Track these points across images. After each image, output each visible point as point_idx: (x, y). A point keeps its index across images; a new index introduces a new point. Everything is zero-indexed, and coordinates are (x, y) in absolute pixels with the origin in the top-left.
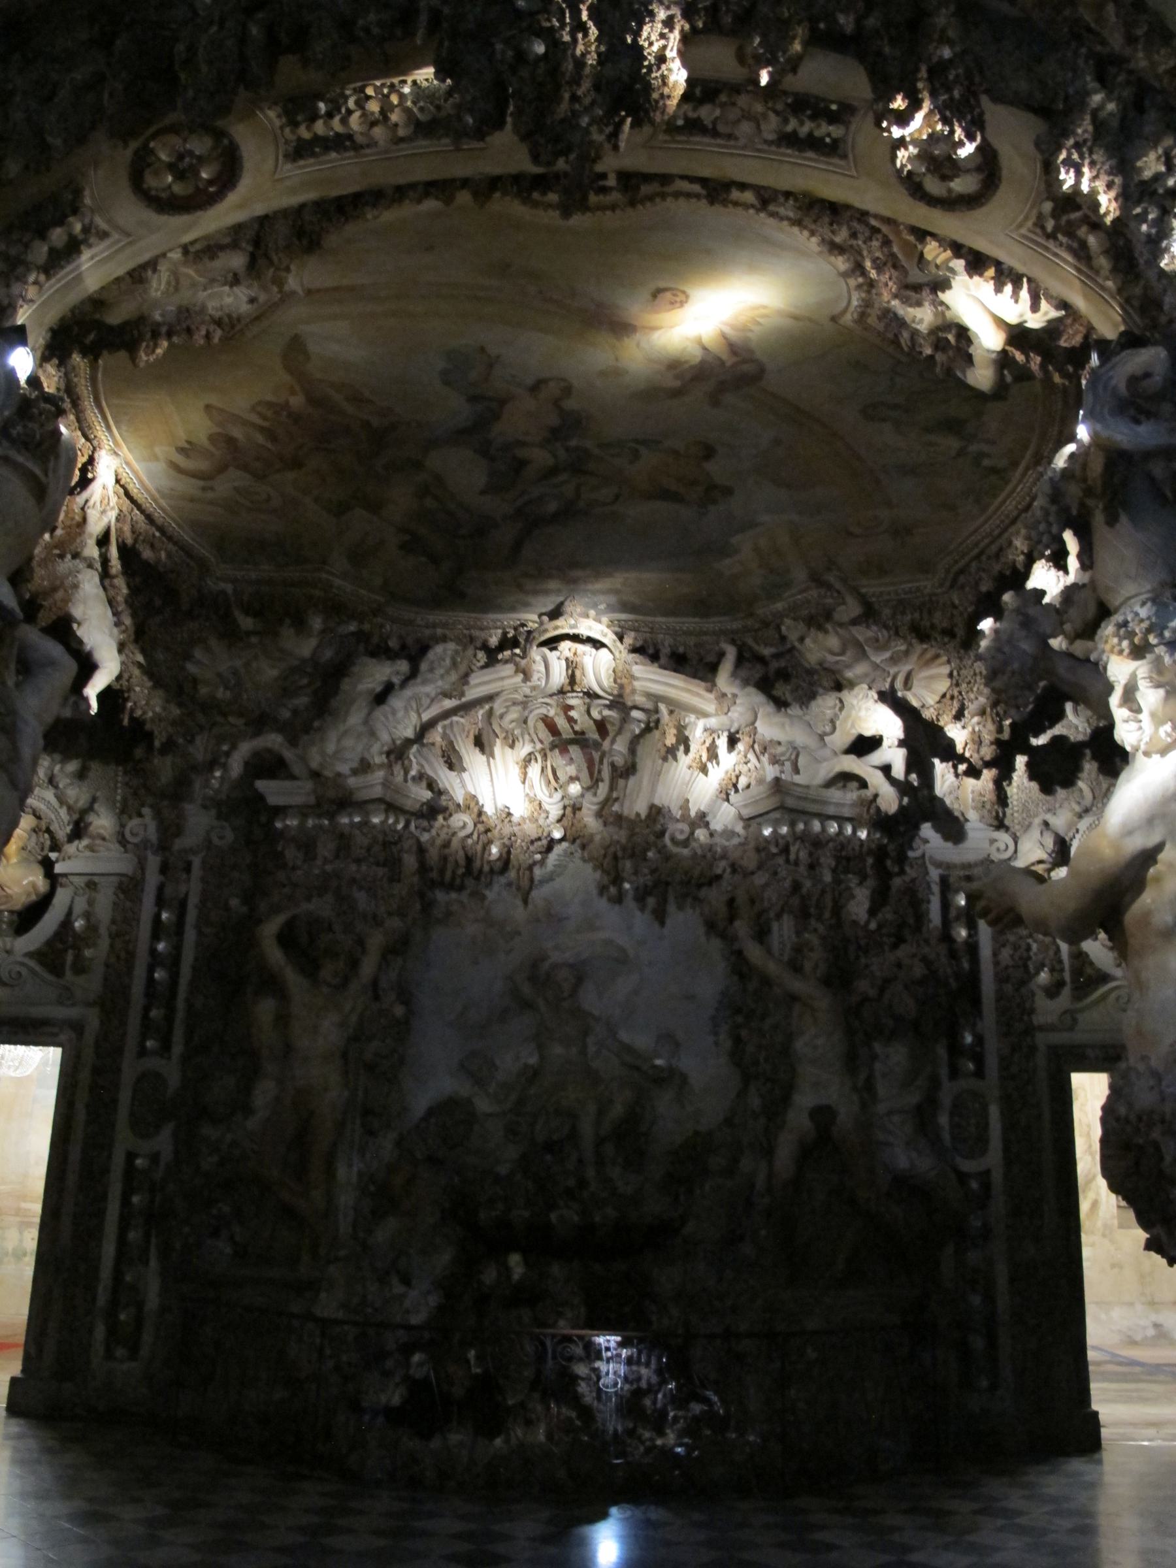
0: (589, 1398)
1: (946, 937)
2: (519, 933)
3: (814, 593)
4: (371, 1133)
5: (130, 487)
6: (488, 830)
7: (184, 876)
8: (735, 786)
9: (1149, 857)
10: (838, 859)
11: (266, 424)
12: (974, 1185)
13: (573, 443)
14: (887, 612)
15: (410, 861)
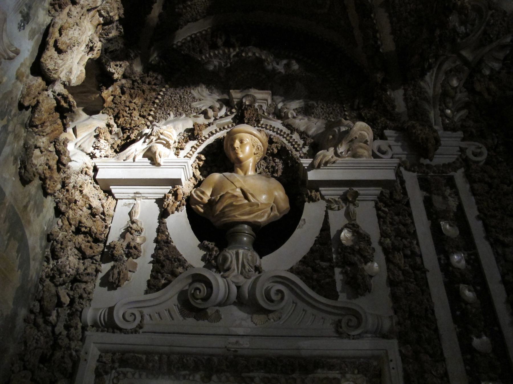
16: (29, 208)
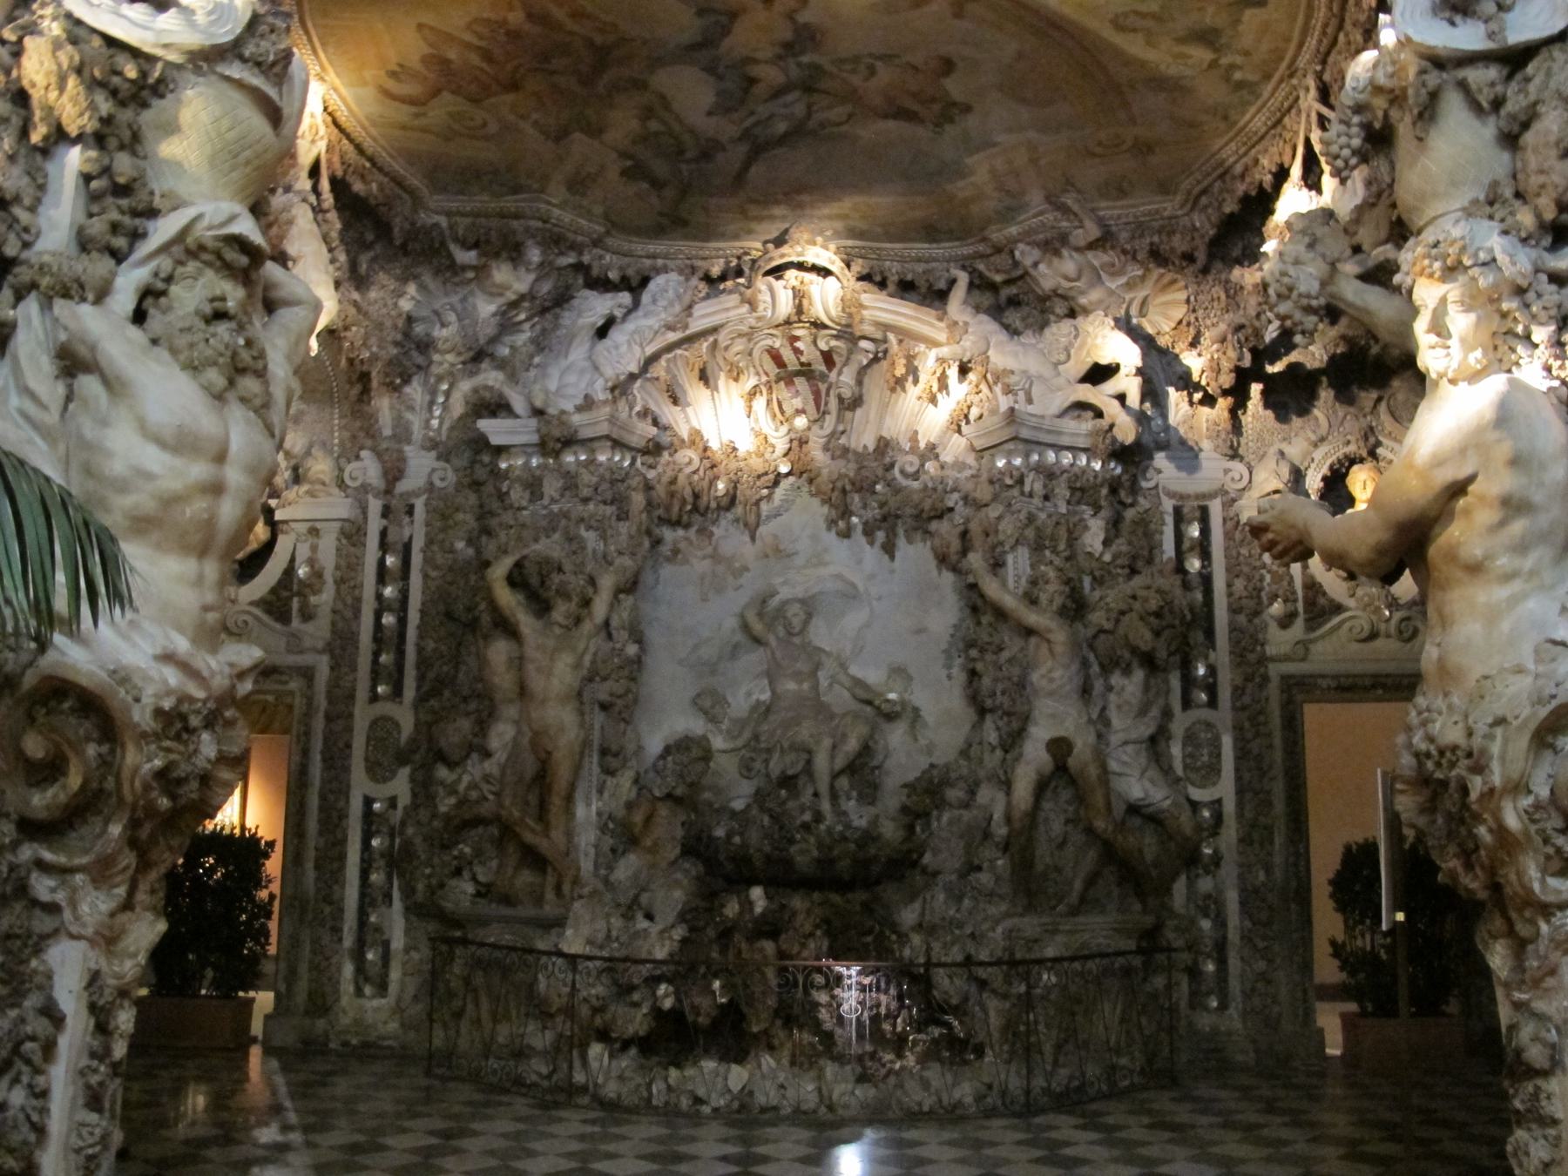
0: (829, 1024)
1: (1180, 569)
2: (747, 569)
3: (1049, 217)
4: (610, 772)
5: (338, 114)
6: (713, 466)
7: (407, 519)
8: (966, 416)
9: (1458, 489)
10: (1073, 489)
11: (483, 44)
12: (1206, 814)
13: (805, 59)
14: (1124, 235)
15: (638, 499)
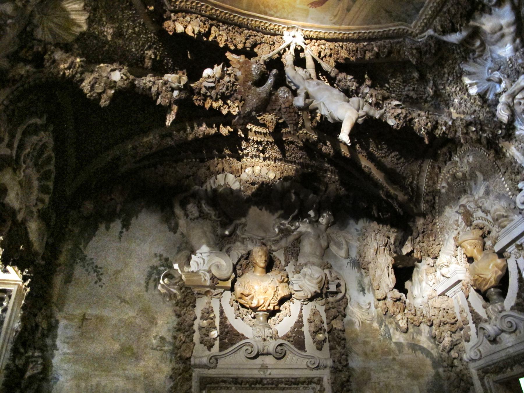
5: (322, 35)
16: (415, 337)
